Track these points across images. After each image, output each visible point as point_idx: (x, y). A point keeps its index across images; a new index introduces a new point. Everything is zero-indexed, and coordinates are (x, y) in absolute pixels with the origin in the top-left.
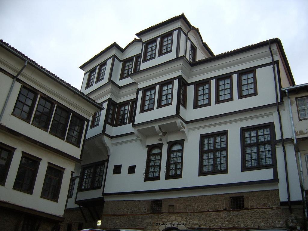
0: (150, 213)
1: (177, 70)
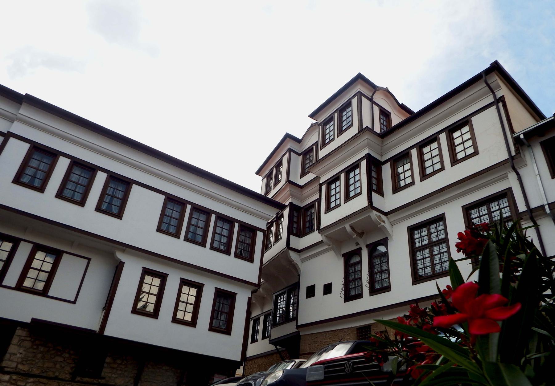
1: (363, 148)
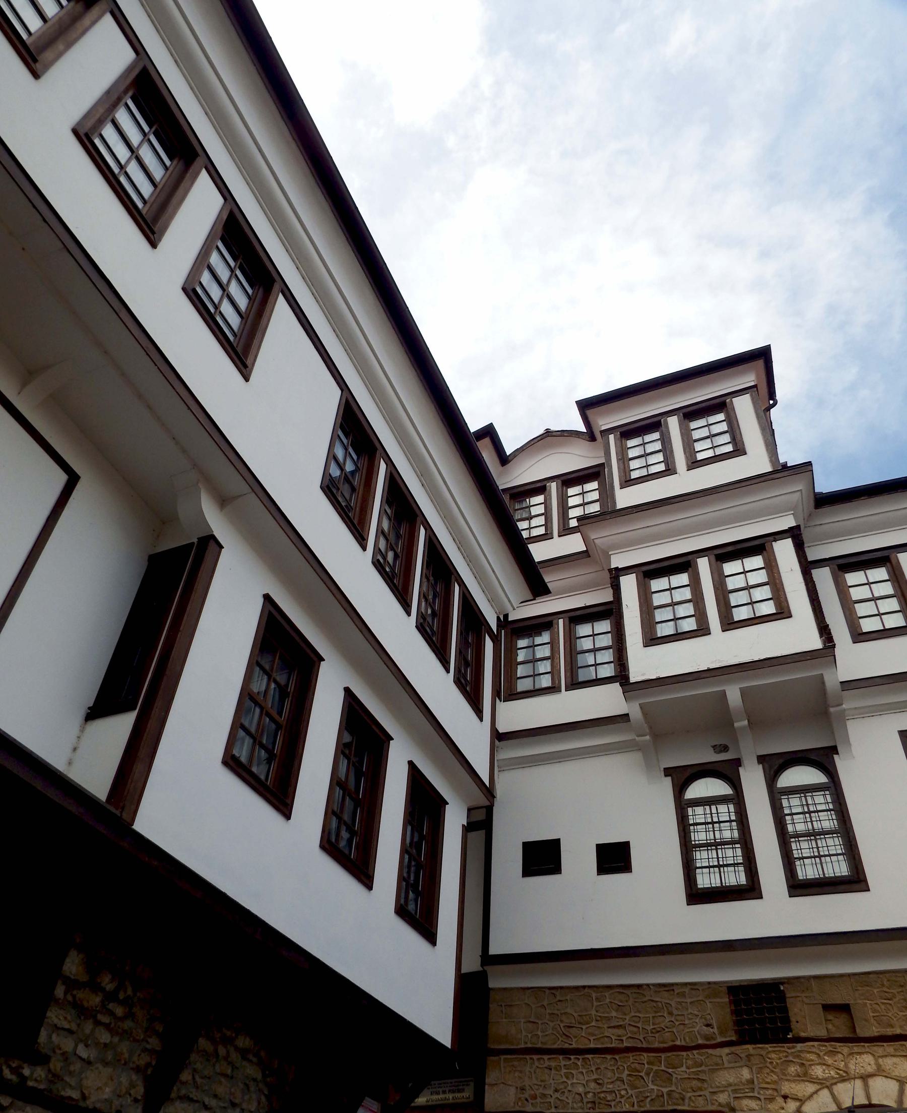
0: (734, 1038)
